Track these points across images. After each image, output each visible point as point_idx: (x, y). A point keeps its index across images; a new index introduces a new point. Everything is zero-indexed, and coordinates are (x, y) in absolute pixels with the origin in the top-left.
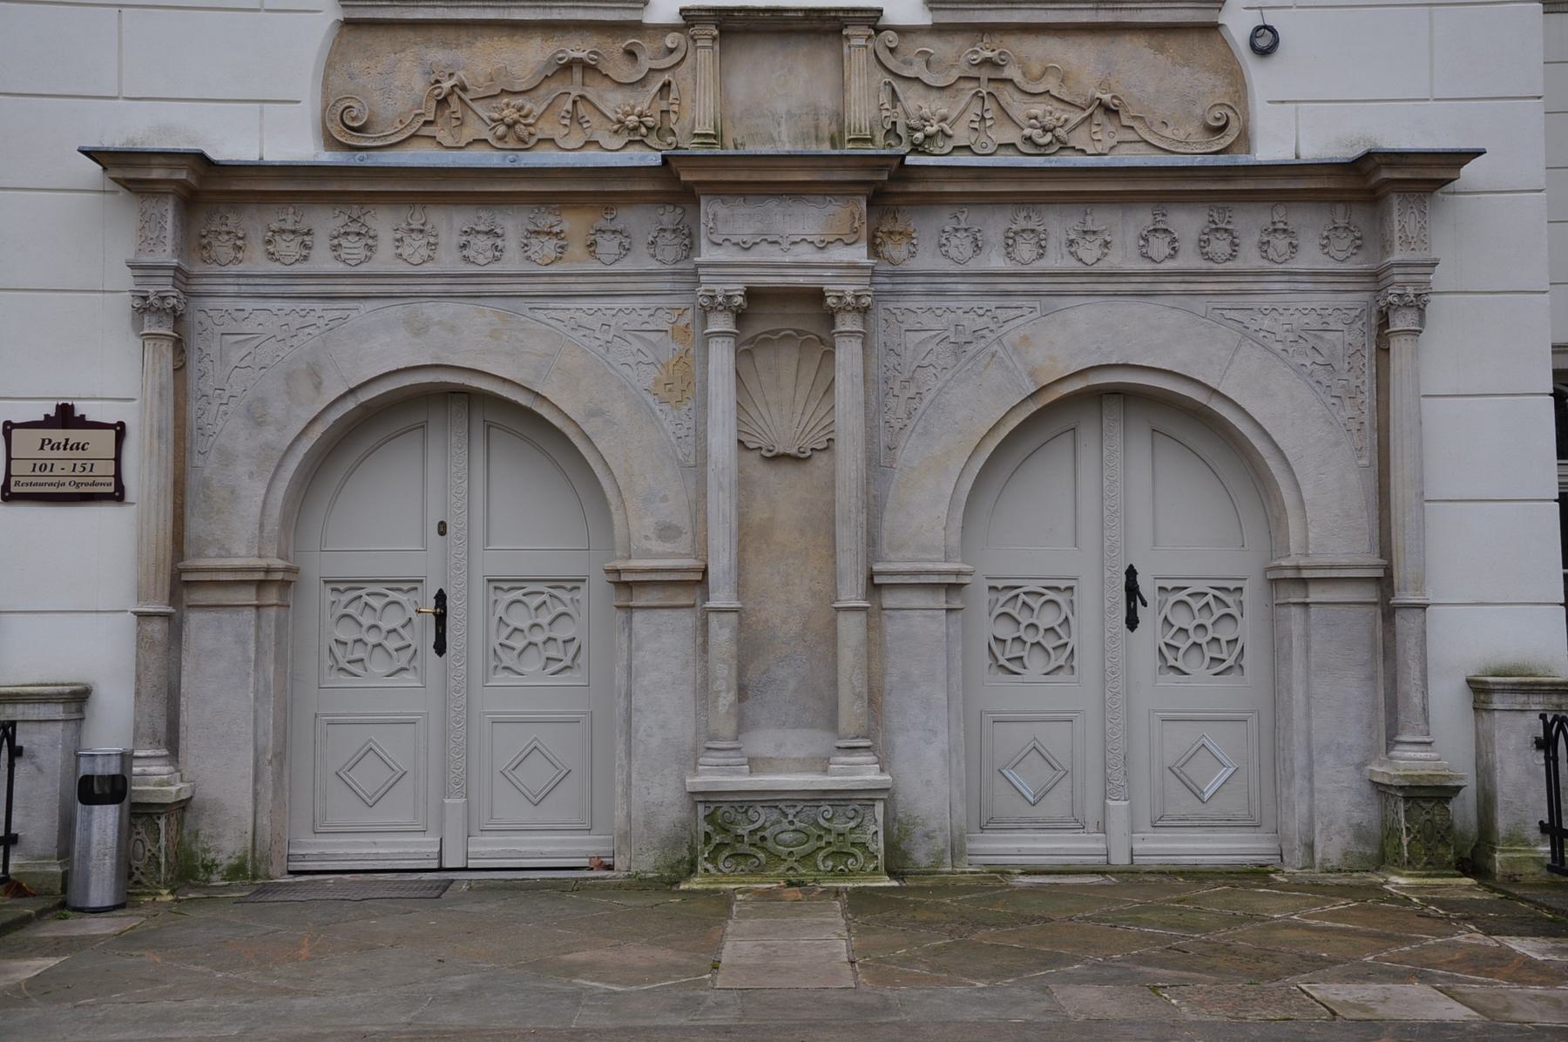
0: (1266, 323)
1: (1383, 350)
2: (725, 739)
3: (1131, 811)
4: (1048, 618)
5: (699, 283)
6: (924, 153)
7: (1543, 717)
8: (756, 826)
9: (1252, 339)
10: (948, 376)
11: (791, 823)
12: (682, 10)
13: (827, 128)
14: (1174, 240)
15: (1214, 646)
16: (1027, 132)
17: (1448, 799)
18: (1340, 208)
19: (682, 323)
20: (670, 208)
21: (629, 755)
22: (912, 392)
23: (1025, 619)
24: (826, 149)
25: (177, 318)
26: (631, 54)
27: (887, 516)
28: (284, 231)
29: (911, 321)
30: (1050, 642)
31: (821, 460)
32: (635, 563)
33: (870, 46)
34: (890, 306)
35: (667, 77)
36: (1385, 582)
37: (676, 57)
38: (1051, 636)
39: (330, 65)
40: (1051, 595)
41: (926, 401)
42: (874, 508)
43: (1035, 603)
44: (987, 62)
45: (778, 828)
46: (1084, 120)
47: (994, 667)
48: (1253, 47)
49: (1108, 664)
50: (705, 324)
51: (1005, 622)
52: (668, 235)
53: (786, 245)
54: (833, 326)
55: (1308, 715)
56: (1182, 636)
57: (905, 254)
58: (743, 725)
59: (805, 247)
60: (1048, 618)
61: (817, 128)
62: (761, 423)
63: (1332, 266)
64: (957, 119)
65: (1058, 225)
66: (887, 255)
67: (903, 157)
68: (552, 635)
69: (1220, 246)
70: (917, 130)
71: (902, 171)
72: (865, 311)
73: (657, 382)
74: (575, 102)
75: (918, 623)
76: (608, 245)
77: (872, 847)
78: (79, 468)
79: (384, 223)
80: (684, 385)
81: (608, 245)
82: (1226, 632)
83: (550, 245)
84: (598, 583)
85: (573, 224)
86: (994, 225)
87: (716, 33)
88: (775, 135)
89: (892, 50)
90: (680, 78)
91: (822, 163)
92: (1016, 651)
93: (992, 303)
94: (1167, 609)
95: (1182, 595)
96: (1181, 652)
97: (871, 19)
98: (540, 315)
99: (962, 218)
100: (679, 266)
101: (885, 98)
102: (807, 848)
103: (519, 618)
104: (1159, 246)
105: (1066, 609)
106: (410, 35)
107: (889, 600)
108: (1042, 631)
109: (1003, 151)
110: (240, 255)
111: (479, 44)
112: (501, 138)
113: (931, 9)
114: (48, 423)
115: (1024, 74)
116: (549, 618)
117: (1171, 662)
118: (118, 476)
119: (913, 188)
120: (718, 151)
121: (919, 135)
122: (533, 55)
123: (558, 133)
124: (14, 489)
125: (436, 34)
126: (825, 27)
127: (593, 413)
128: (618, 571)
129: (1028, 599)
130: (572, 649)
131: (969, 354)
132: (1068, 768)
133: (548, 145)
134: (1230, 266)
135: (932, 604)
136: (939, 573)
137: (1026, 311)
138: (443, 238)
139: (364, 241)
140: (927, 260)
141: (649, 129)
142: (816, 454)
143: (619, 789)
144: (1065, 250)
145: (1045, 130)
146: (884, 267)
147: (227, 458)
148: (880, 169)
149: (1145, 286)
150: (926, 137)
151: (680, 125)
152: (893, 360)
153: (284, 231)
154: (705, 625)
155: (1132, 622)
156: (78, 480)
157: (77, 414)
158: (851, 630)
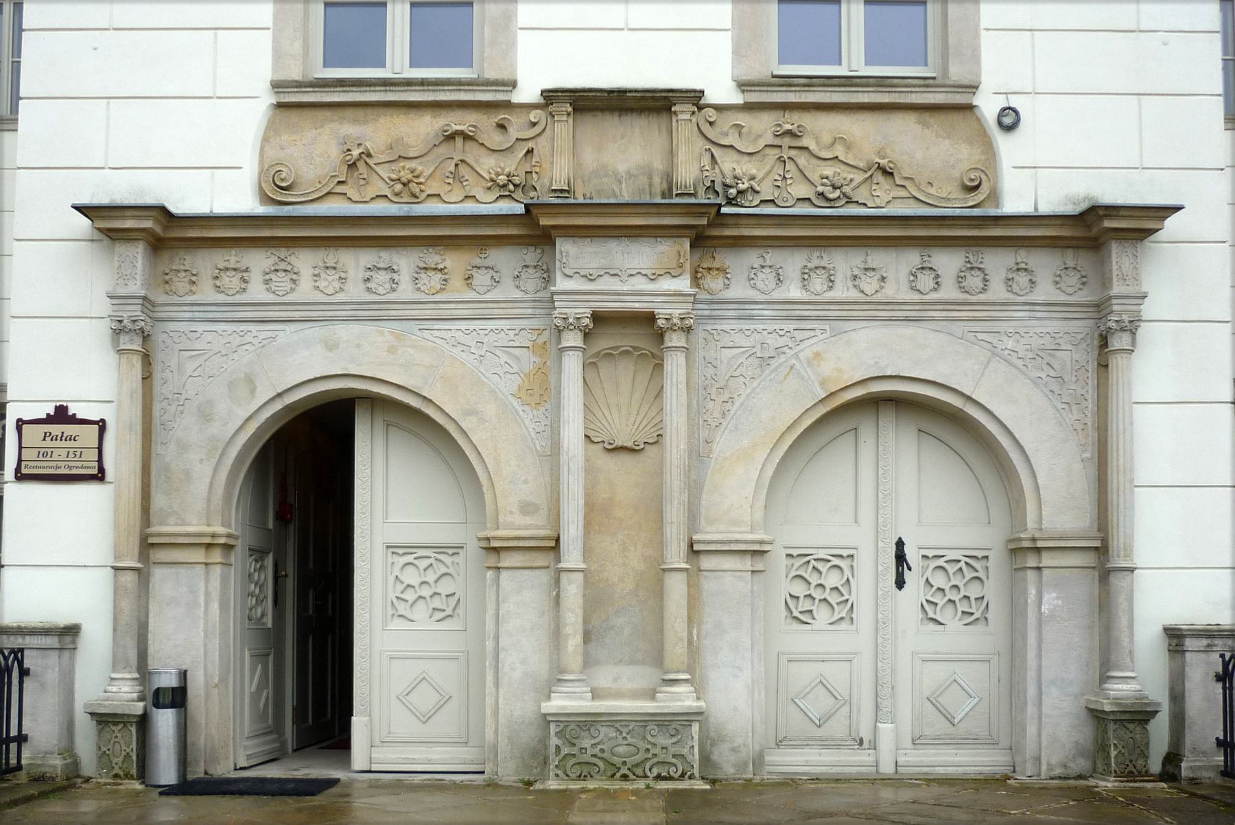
0: (1010, 344)
1: (1103, 366)
2: (571, 673)
3: (897, 732)
4: (833, 580)
5: (555, 308)
6: (736, 205)
7: (1222, 656)
8: (597, 740)
9: (995, 359)
10: (755, 384)
11: (625, 738)
12: (542, 92)
13: (659, 184)
14: (938, 276)
15: (965, 602)
16: (820, 189)
17: (1147, 721)
18: (1070, 252)
19: (540, 341)
20: (531, 249)
21: (497, 684)
22: (726, 397)
23: (814, 579)
24: (659, 200)
25: (146, 338)
26: (502, 127)
27: (704, 496)
28: (227, 269)
29: (726, 340)
30: (834, 599)
31: (651, 451)
32: (500, 533)
33: (694, 120)
34: (709, 327)
35: (530, 145)
36: (1102, 550)
37: (537, 129)
38: (835, 594)
39: (265, 139)
40: (836, 561)
41: (737, 404)
42: (694, 489)
43: (822, 567)
44: (789, 133)
45: (614, 743)
46: (867, 179)
47: (790, 620)
48: (1000, 124)
49: (880, 616)
50: (559, 342)
51: (799, 582)
52: (531, 270)
53: (624, 278)
54: (662, 342)
55: (1039, 656)
56: (940, 594)
57: (721, 285)
58: (588, 663)
59: (640, 279)
60: (833, 580)
61: (650, 185)
62: (604, 421)
63: (1063, 298)
64: (763, 179)
65: (844, 262)
66: (706, 287)
67: (720, 206)
68: (438, 591)
69: (974, 281)
70: (731, 187)
71: (719, 219)
72: (688, 330)
73: (520, 388)
74: (456, 165)
75: (727, 581)
76: (481, 278)
77: (689, 758)
78: (71, 455)
79: (305, 261)
80: (542, 390)
81: (481, 278)
82: (974, 591)
83: (437, 278)
84: (473, 547)
85: (454, 261)
86: (793, 262)
87: (570, 109)
88: (617, 190)
89: (711, 123)
90: (541, 146)
91: (654, 210)
92: (805, 605)
93: (791, 326)
94: (928, 573)
95: (941, 562)
96: (939, 607)
97: (695, 98)
98: (426, 334)
99: (767, 257)
100: (539, 295)
101: (706, 160)
102: (638, 758)
103: (411, 577)
104: (926, 281)
105: (847, 572)
106: (328, 113)
107: (707, 563)
108: (828, 590)
109: (800, 204)
110: (194, 288)
111: (382, 121)
112: (397, 194)
113: (743, 91)
114: (49, 420)
115: (817, 143)
116: (435, 577)
117: (931, 615)
118: (100, 460)
119: (728, 232)
120: (571, 201)
121: (733, 191)
122: (426, 127)
123: (442, 190)
124: (24, 471)
125: (349, 112)
126: (655, 104)
127: (469, 413)
128: (488, 539)
129: (819, 566)
130: (453, 602)
131: (773, 366)
132: (847, 698)
133: (435, 199)
134: (982, 297)
135: (740, 567)
136: (746, 542)
137: (818, 332)
138: (351, 273)
139: (290, 276)
140: (738, 290)
141: (515, 186)
142: (647, 446)
143: (488, 711)
144: (850, 284)
145: (835, 188)
146: (703, 296)
147: (184, 447)
148: (701, 215)
150: (739, 192)
151: (542, 183)
152: (711, 371)
153: (227, 269)
154: (557, 581)
155: (900, 583)
156: (71, 464)
157: (70, 413)
158: (676, 587)
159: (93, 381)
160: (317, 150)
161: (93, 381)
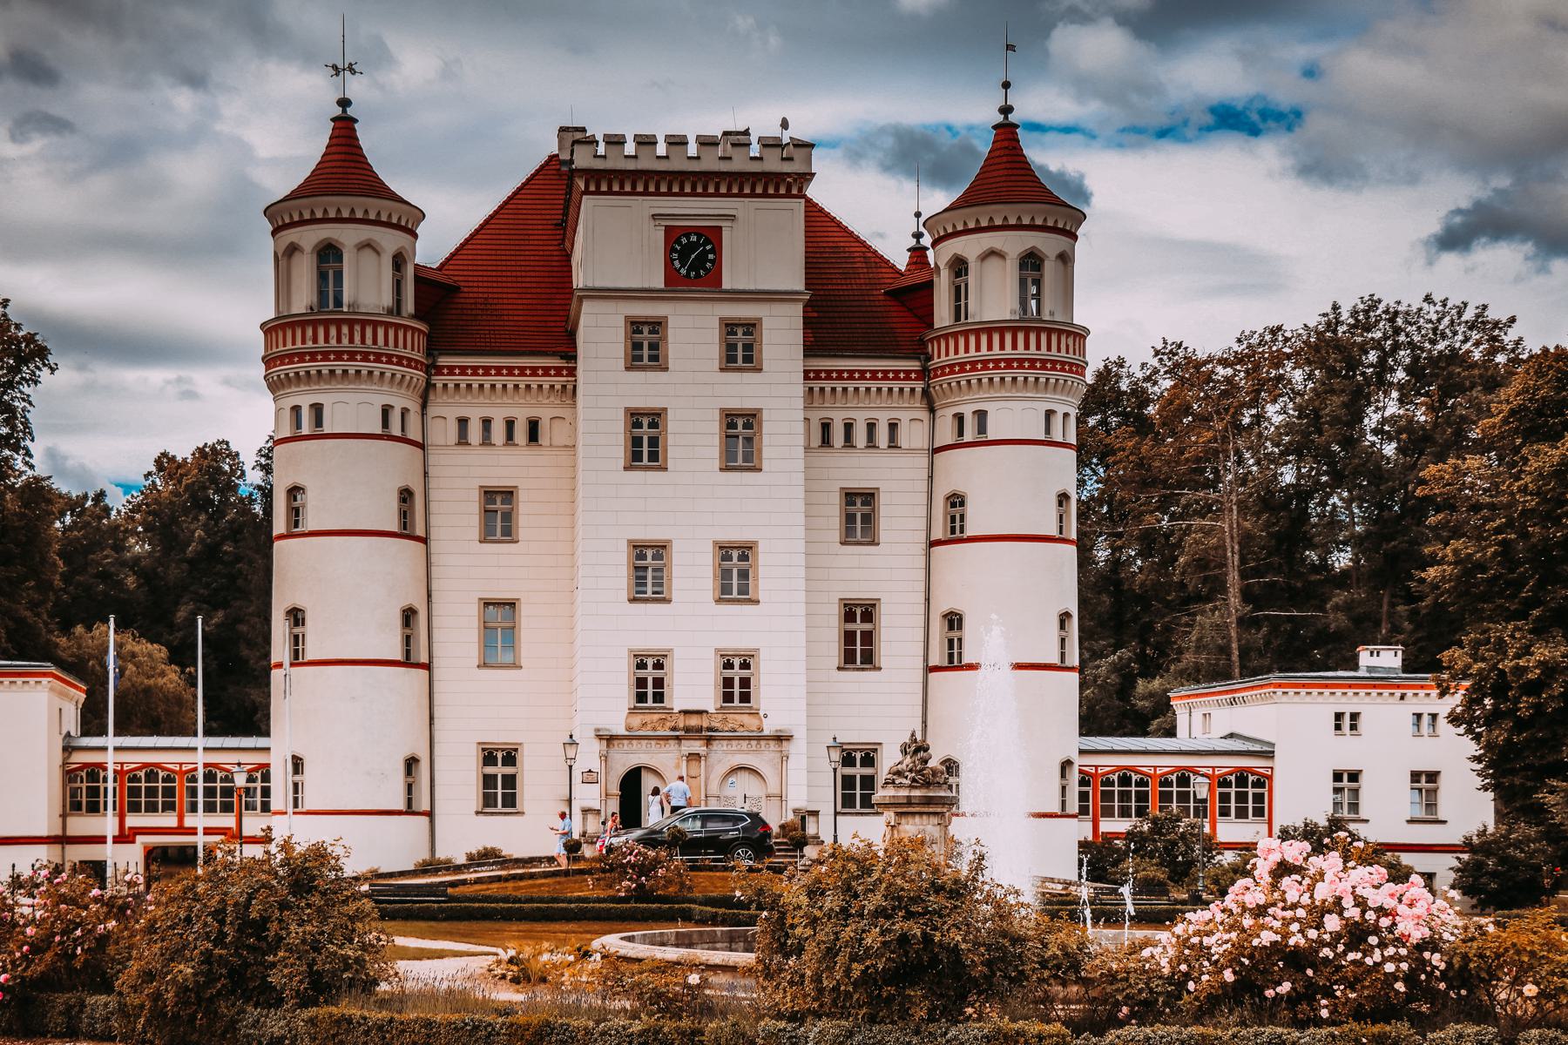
9: (762, 759)
122: (656, 717)
126: (700, 712)
149: (748, 752)
159: (596, 765)
160: (636, 721)
161: (596, 765)
